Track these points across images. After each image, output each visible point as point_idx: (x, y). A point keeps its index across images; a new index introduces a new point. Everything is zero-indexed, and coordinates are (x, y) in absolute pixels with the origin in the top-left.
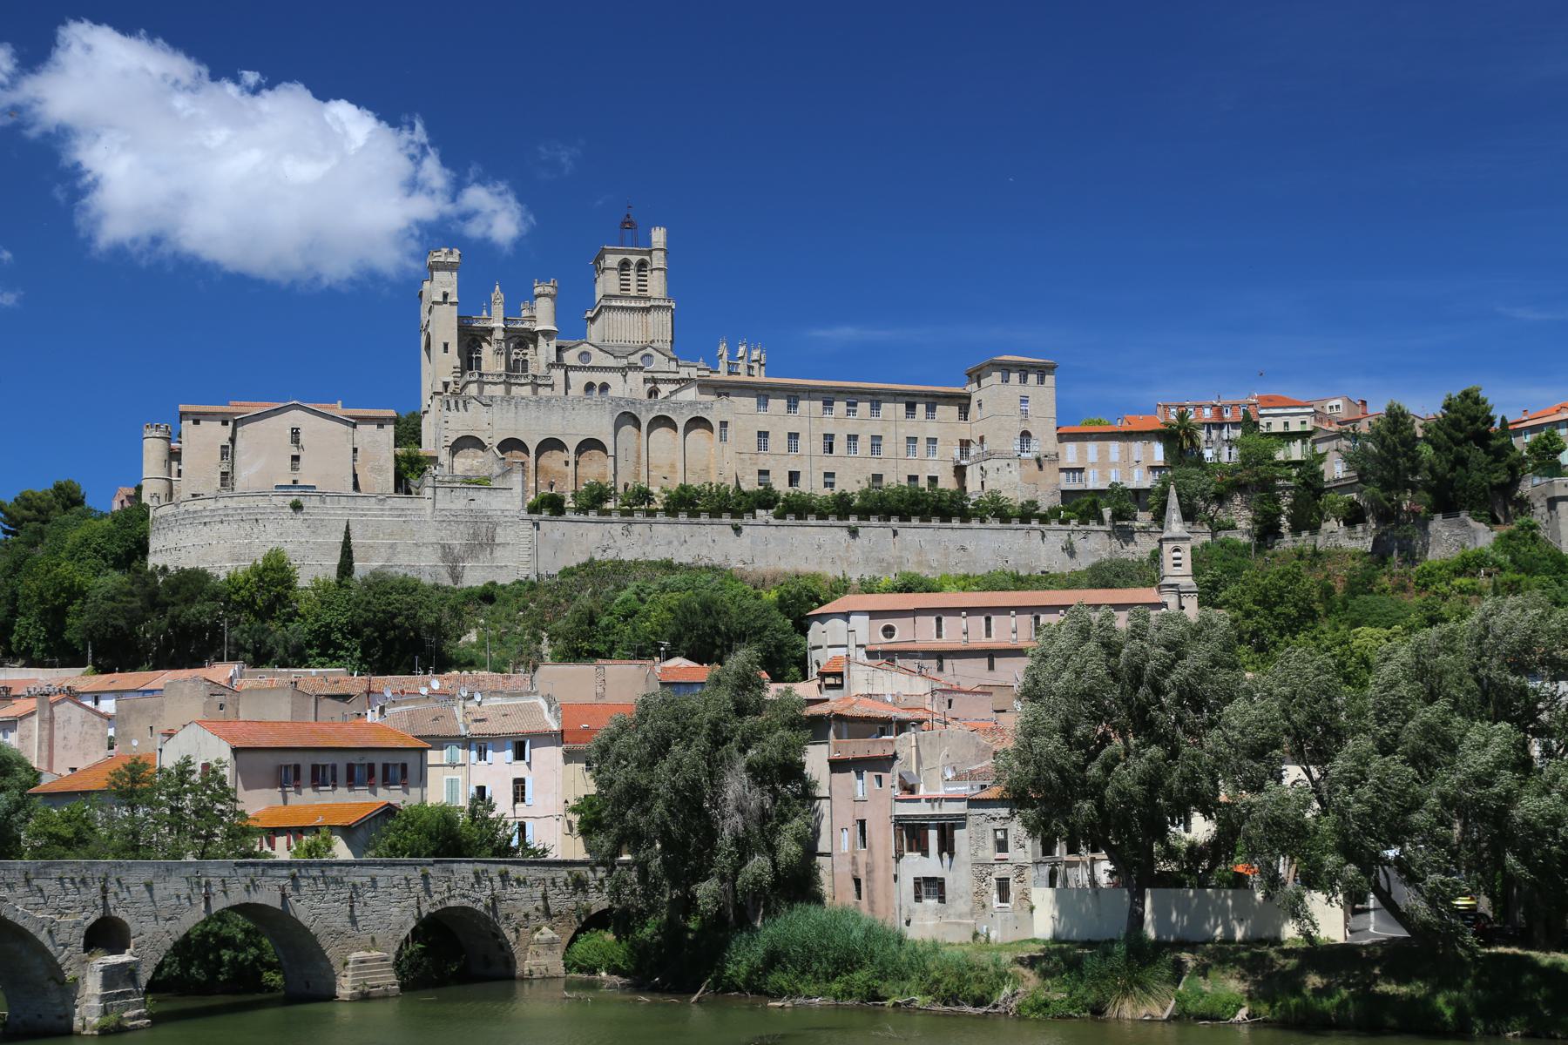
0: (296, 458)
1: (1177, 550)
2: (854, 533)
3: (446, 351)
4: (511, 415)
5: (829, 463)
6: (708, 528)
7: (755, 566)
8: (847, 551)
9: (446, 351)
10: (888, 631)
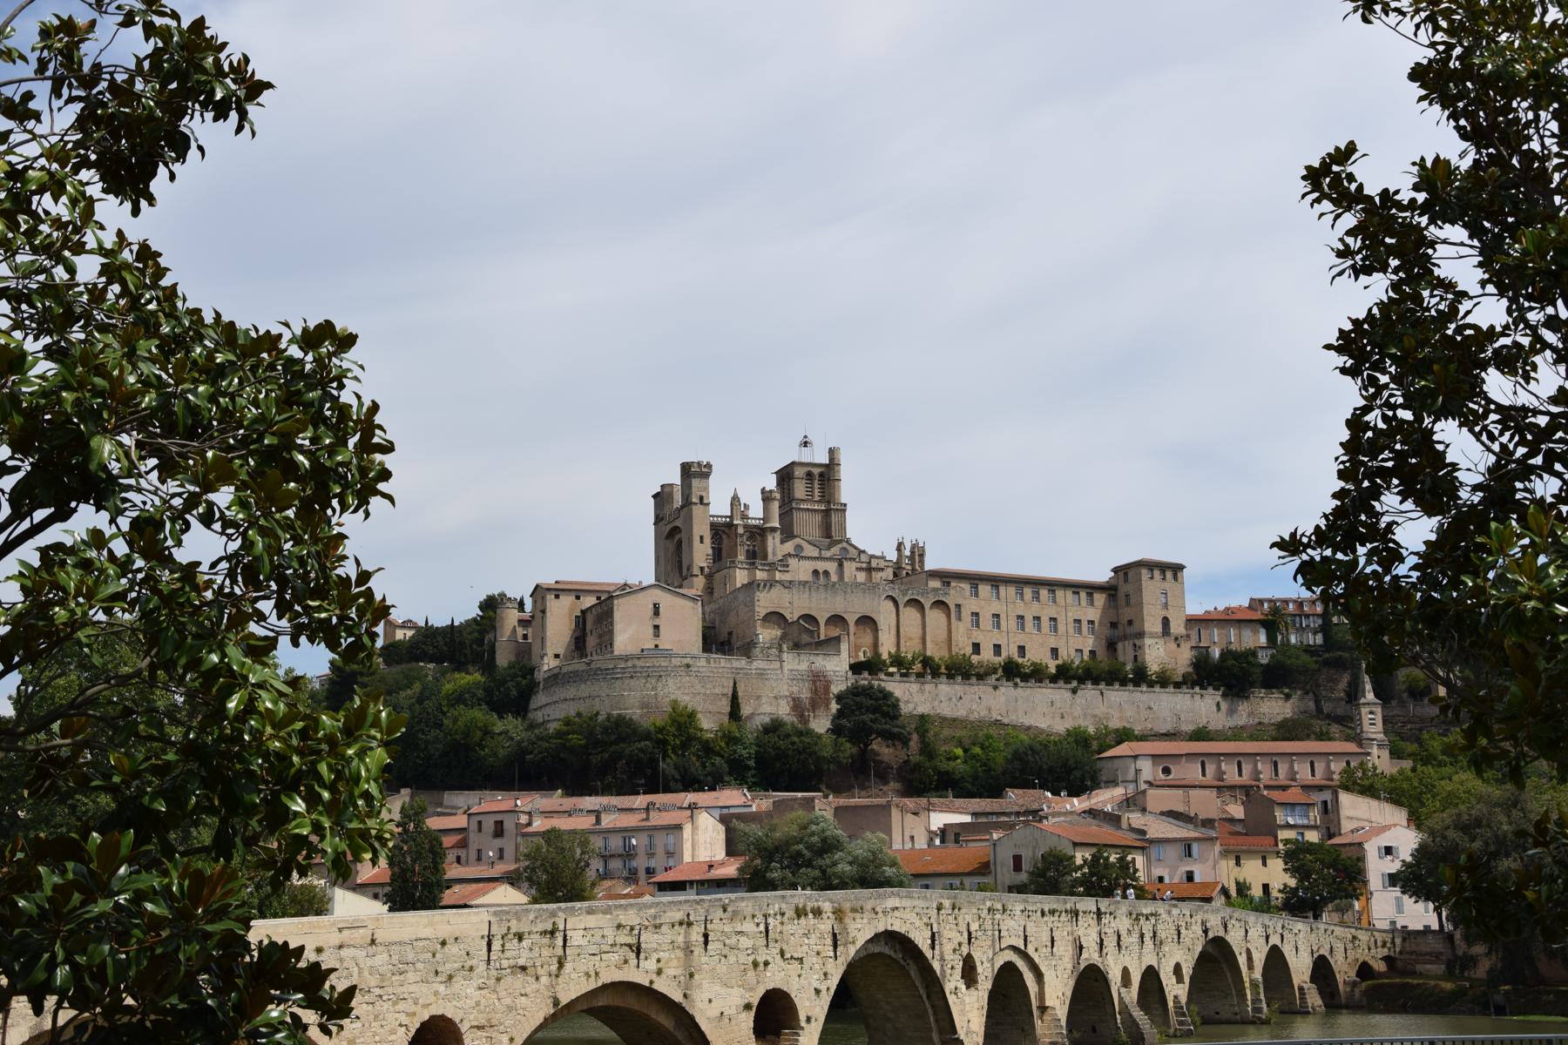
0: (657, 627)
1: (1371, 713)
2: (1074, 691)
3: (702, 542)
4: (806, 596)
5: (1020, 639)
9: (702, 542)
10: (1166, 771)
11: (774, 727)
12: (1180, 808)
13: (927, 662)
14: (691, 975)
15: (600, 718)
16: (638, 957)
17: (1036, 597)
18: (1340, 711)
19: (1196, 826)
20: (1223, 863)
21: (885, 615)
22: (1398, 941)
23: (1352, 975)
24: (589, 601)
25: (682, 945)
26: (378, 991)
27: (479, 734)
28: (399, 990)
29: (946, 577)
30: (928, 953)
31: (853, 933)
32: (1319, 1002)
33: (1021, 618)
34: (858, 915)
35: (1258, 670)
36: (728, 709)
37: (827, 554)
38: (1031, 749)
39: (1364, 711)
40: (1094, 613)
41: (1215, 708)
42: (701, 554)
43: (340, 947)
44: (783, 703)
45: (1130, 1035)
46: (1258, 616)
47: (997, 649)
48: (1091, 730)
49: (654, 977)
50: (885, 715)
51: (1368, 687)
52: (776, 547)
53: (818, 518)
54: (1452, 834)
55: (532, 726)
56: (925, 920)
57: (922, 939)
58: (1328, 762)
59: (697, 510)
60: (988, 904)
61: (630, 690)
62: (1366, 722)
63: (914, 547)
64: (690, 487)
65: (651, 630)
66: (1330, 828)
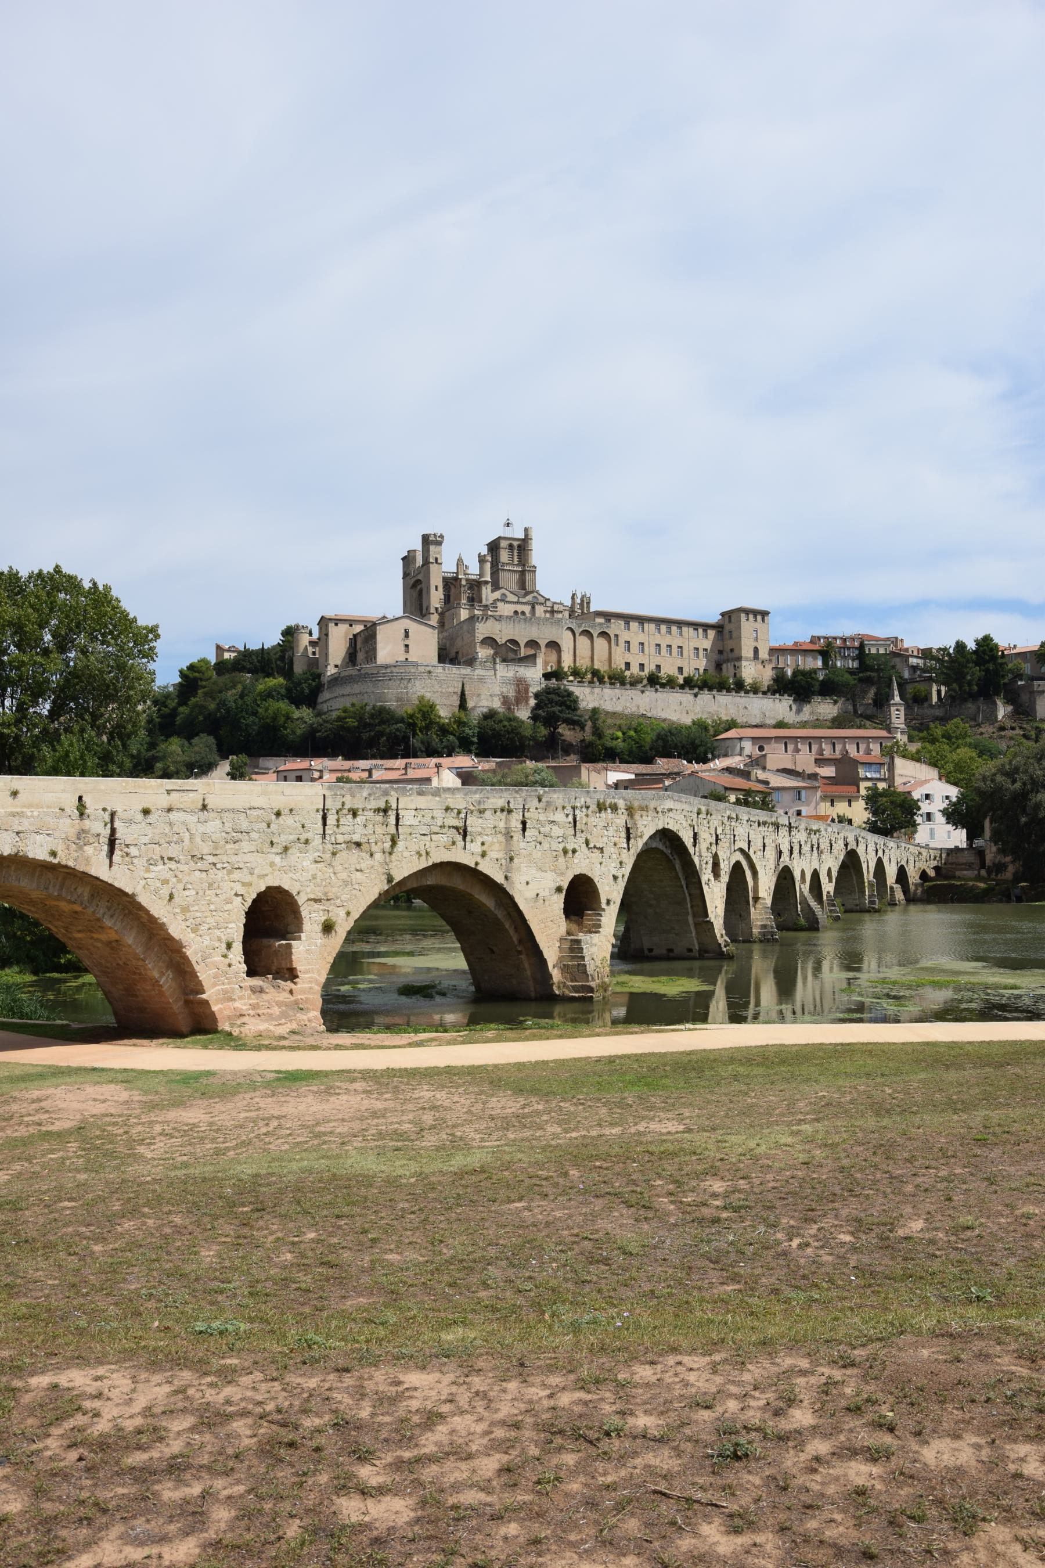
0: (407, 646)
2: (696, 695)
4: (512, 626)
5: (657, 660)
6: (629, 692)
11: (490, 715)
12: (790, 766)
13: (595, 673)
14: (511, 859)
15: (368, 708)
16: (464, 839)
18: (869, 712)
19: (803, 779)
20: (822, 804)
21: (566, 641)
22: (944, 856)
23: (917, 878)
24: (358, 628)
25: (503, 830)
26: (211, 859)
27: (283, 719)
28: (233, 859)
29: (608, 616)
30: (691, 850)
31: (641, 829)
32: (902, 897)
33: (658, 645)
34: (644, 813)
35: (817, 684)
36: (458, 703)
37: (521, 600)
38: (670, 732)
39: (893, 709)
40: (707, 644)
42: (436, 598)
43: (169, 810)
44: (496, 699)
45: (807, 920)
46: (816, 647)
47: (642, 666)
48: (709, 721)
49: (479, 859)
50: (569, 707)
51: (896, 692)
52: (488, 595)
53: (516, 576)
54: (999, 778)
55: (319, 714)
56: (690, 822)
57: (687, 839)
58: (869, 743)
59: (433, 568)
60: (728, 812)
61: (389, 689)
62: (893, 717)
63: (583, 597)
64: (428, 551)
65: (403, 648)
66: (890, 779)
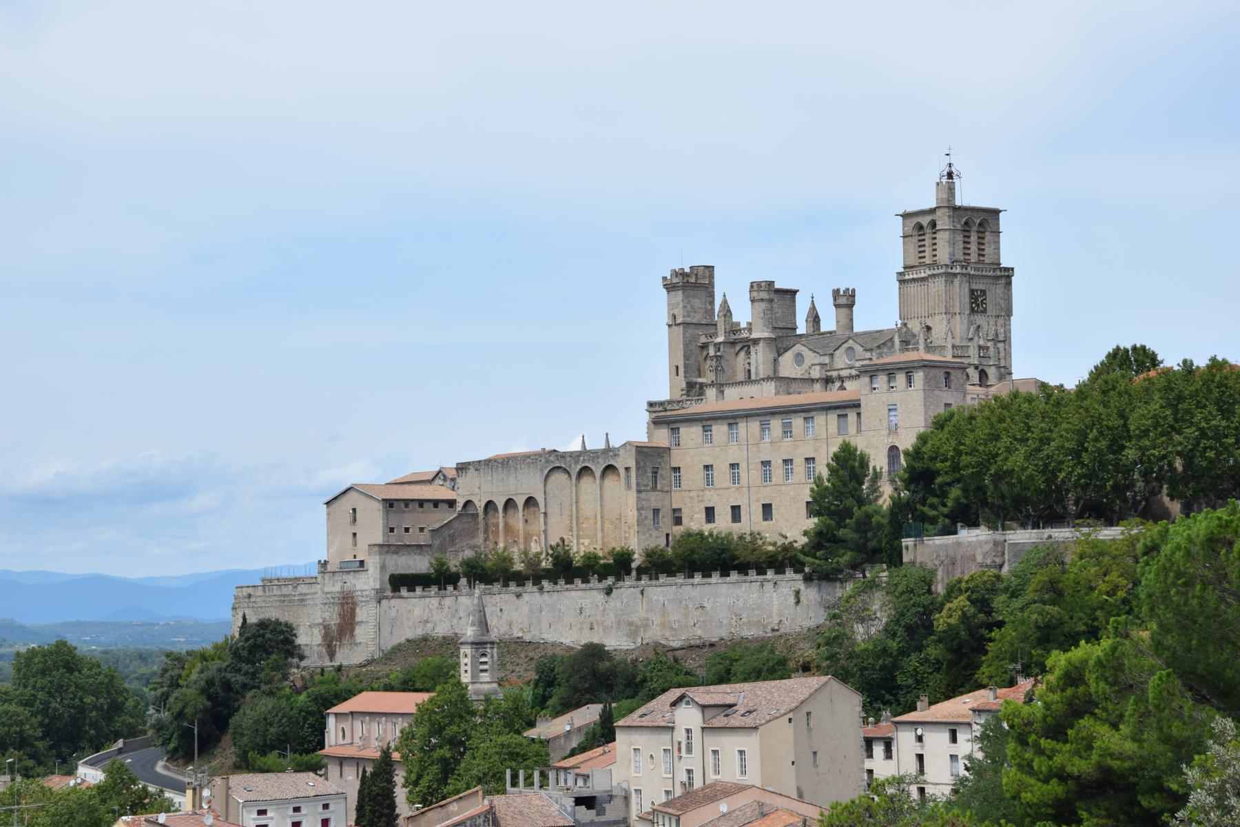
0: (355, 534)
3: (677, 375)
4: (490, 478)
7: (533, 633)
8: (603, 615)
17: (787, 431)
33: (766, 464)
41: (792, 600)
47: (736, 511)
